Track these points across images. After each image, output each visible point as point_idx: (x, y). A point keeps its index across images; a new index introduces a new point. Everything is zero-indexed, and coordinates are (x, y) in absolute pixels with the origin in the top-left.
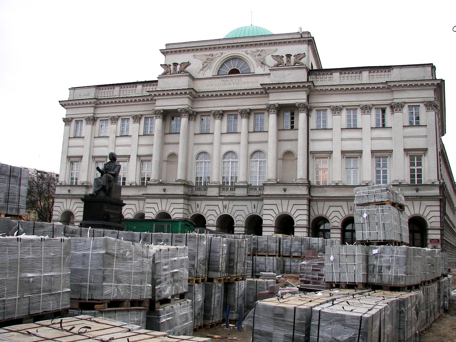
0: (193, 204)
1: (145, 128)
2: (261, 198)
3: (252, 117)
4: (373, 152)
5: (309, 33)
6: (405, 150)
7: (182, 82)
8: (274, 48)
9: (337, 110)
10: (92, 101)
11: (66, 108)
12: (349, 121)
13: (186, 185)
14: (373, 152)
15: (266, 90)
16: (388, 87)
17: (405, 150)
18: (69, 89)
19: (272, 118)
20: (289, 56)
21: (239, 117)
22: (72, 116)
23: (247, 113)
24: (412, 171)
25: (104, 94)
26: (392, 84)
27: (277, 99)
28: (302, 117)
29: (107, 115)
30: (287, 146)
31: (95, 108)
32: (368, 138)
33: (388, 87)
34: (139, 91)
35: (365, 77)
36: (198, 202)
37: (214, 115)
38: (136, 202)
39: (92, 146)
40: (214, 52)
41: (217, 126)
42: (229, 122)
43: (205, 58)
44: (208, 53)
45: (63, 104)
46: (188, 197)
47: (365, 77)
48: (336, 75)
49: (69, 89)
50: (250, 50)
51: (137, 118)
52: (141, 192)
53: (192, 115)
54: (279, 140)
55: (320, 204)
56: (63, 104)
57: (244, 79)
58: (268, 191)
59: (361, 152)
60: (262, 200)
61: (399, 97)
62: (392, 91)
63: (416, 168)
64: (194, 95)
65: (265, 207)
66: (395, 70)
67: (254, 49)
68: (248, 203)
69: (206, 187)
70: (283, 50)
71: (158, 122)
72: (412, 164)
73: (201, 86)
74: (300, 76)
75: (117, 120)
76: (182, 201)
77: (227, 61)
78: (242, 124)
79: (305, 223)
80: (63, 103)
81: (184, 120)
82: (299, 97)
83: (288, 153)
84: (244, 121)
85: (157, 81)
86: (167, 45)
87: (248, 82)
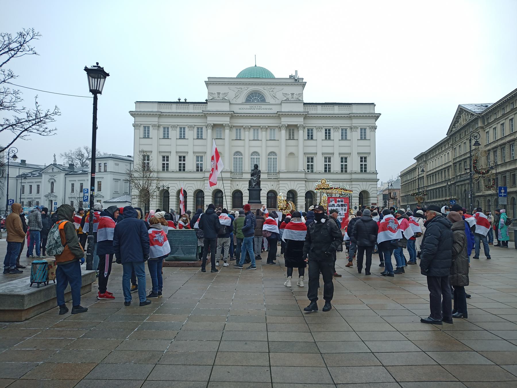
0: (234, 183)
1: (198, 134)
2: (278, 180)
3: (269, 130)
4: (340, 154)
5: (303, 79)
6: (358, 153)
7: (225, 107)
8: (281, 87)
9: (319, 128)
10: (158, 113)
11: (134, 117)
12: (326, 136)
13: (231, 172)
14: (340, 154)
15: (279, 115)
16: (350, 117)
17: (358, 153)
18: (135, 103)
19: (283, 132)
20: (293, 94)
21: (260, 130)
22: (141, 123)
23: (266, 128)
24: (361, 165)
25: (165, 109)
26: (353, 115)
27: (286, 121)
28: (301, 132)
29: (169, 124)
30: (292, 150)
31: (159, 118)
32: (336, 146)
33: (350, 117)
34: (191, 109)
35: (336, 110)
36: (237, 183)
37: (244, 128)
38: (195, 182)
39: (159, 145)
40: (243, 87)
41: (247, 135)
42: (254, 133)
43: (236, 90)
44: (239, 87)
45: (132, 113)
46: (232, 180)
47: (336, 110)
48: (319, 107)
49: (135, 103)
50: (266, 87)
51: (191, 127)
52: (199, 175)
53: (231, 128)
54: (286, 146)
55: (310, 183)
56: (132, 113)
57: (263, 107)
58: (282, 176)
59: (333, 154)
60: (279, 181)
61: (356, 122)
62: (352, 119)
63: (363, 163)
64: (233, 115)
65: (280, 185)
66: (354, 106)
67: (269, 87)
68: (268, 183)
69: (242, 173)
70: (289, 90)
71: (210, 131)
72: (361, 161)
73: (236, 109)
74: (300, 108)
75: (176, 127)
76: (229, 182)
77: (252, 94)
78: (263, 135)
79: (304, 194)
80: (133, 113)
81: (227, 131)
82: (299, 121)
83: (291, 154)
84: (264, 133)
85: (206, 103)
86: (209, 78)
87: (266, 109)
